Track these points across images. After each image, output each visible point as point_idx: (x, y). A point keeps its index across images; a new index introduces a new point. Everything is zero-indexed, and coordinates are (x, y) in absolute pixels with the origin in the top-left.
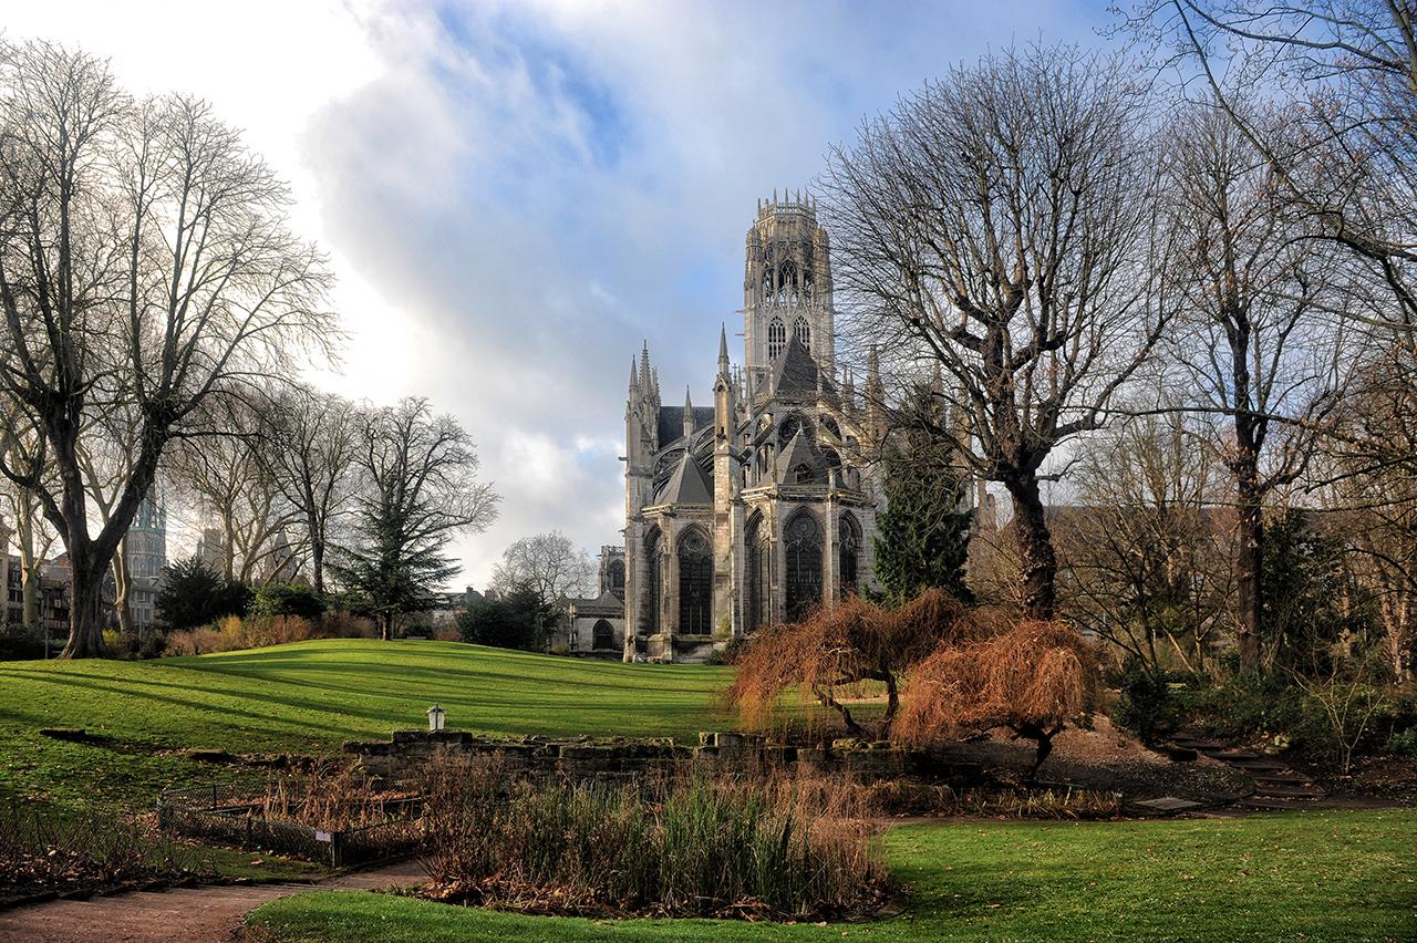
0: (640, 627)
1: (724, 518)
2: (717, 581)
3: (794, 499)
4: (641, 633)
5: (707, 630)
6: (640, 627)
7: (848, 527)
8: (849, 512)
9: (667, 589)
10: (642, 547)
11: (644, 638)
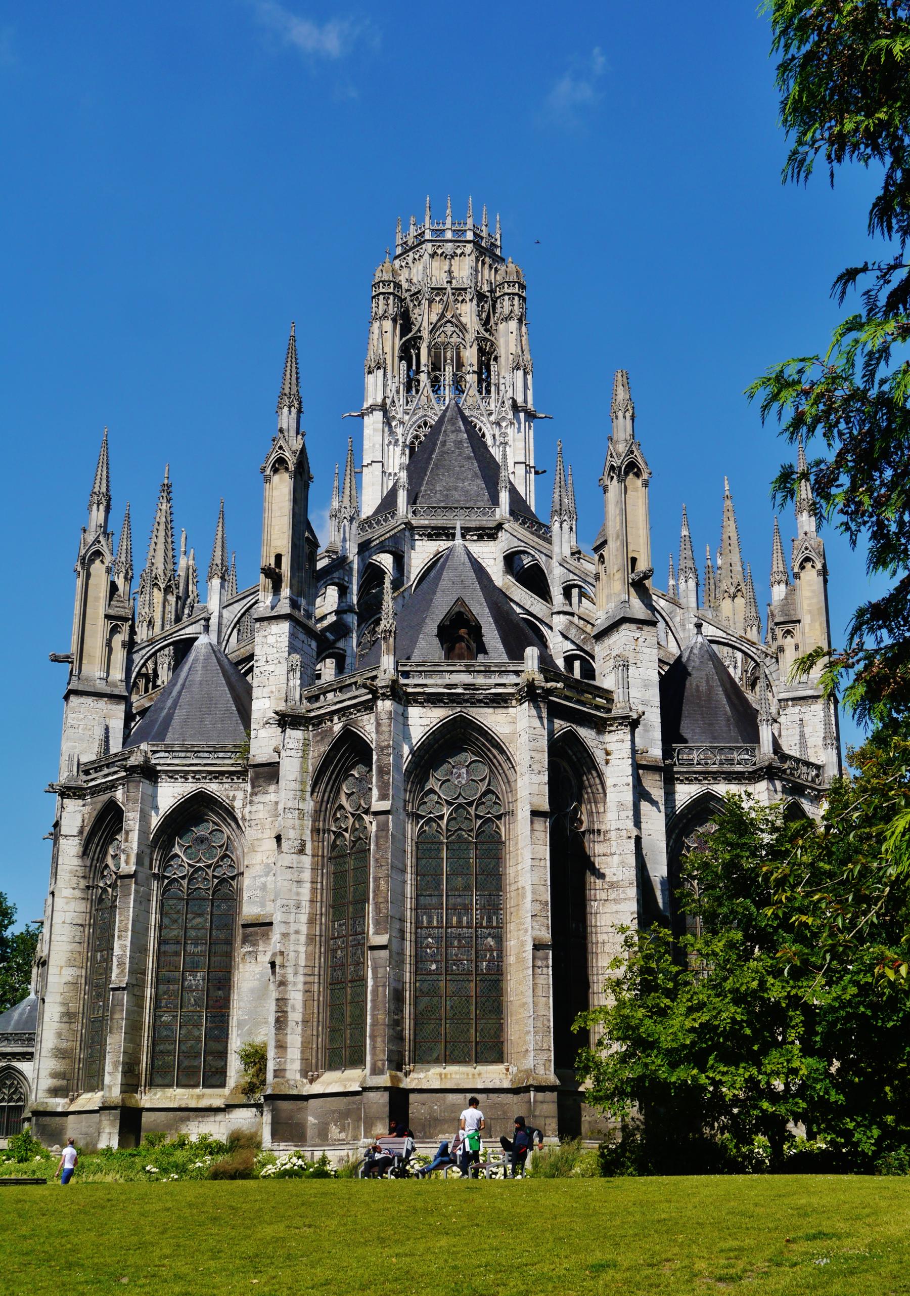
0: (55, 1075)
1: (269, 773)
2: (245, 940)
3: (434, 700)
4: (55, 1092)
5: (215, 1077)
6: (55, 1075)
7: (570, 772)
8: (571, 738)
9: (121, 964)
10: (77, 862)
11: (59, 1104)
